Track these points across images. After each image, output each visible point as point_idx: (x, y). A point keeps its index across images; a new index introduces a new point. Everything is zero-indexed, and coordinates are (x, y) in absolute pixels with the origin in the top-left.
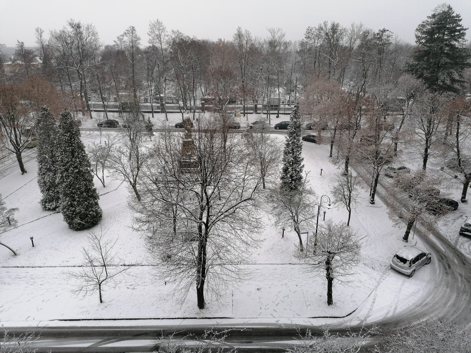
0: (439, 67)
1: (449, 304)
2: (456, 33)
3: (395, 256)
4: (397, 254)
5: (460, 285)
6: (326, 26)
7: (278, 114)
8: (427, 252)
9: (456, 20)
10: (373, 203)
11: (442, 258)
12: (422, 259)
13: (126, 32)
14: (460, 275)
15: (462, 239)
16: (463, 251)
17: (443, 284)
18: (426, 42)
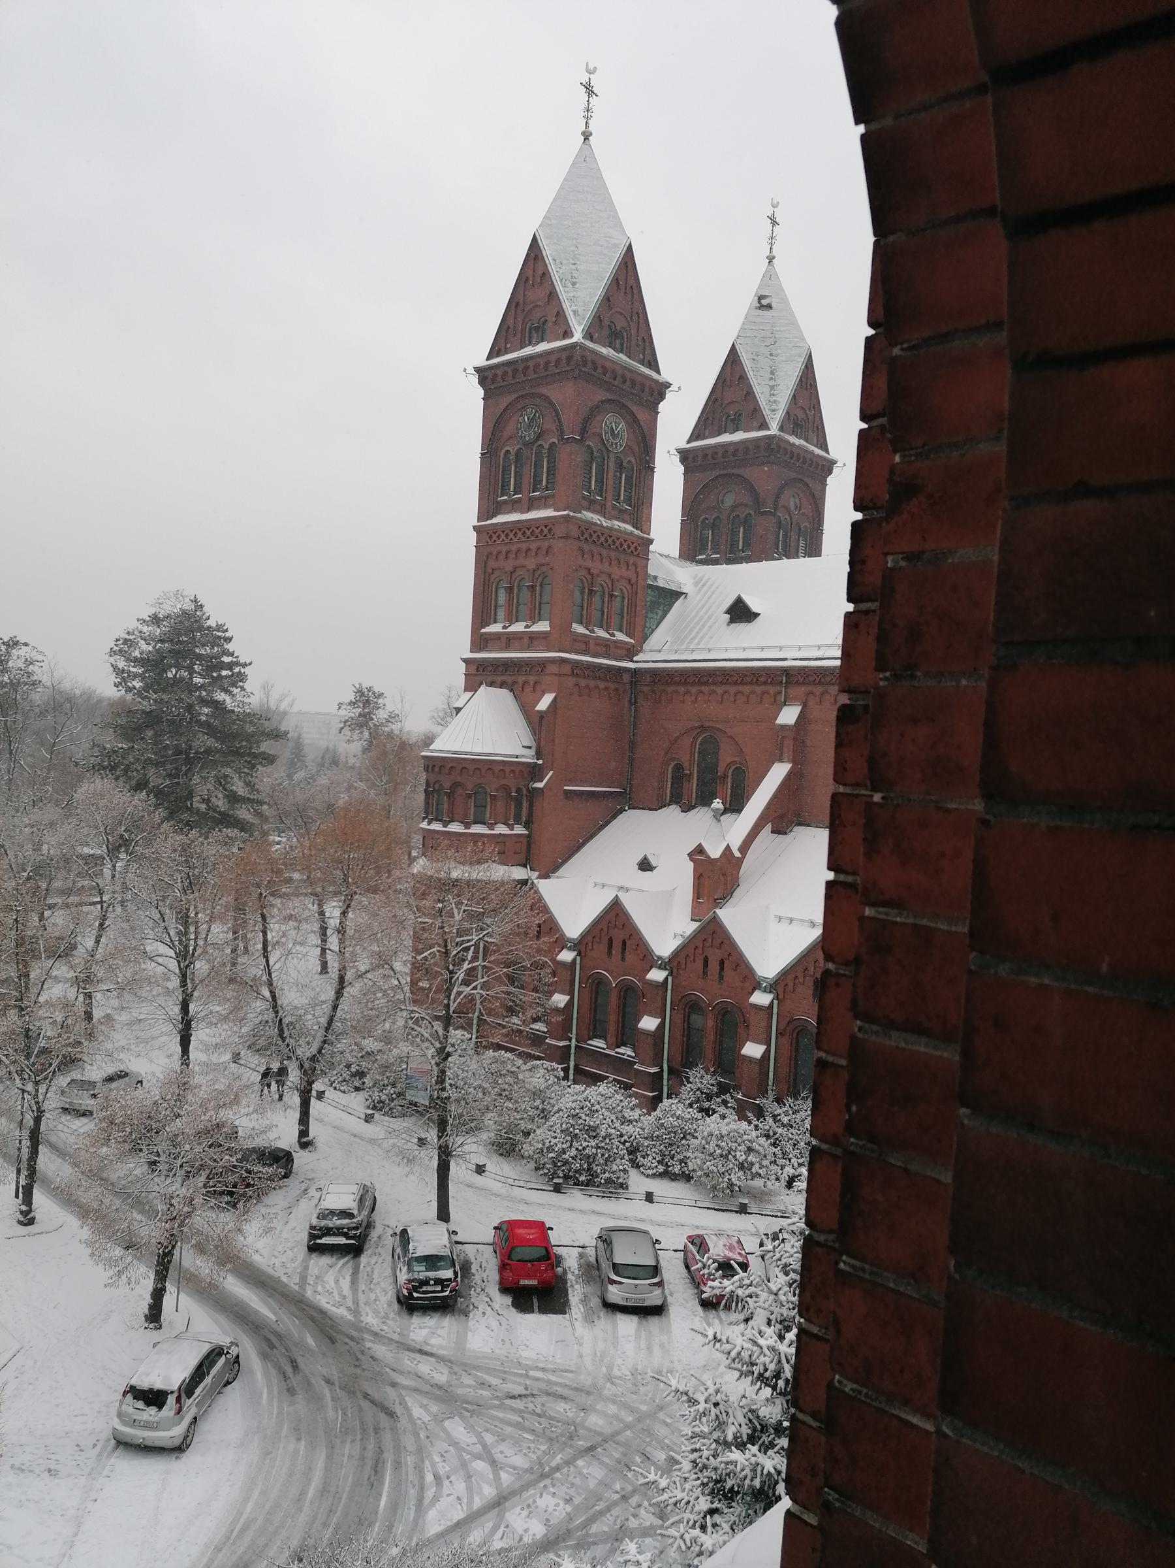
0: (189, 760)
1: (311, 1492)
2: (224, 673)
3: (125, 1393)
4: (133, 1382)
5: (331, 1414)
8: (224, 1341)
9: (218, 637)
10: (31, 1222)
11: (272, 1346)
12: (214, 1371)
14: (328, 1381)
15: (320, 1263)
16: (323, 1302)
17: (284, 1434)
18: (146, 688)
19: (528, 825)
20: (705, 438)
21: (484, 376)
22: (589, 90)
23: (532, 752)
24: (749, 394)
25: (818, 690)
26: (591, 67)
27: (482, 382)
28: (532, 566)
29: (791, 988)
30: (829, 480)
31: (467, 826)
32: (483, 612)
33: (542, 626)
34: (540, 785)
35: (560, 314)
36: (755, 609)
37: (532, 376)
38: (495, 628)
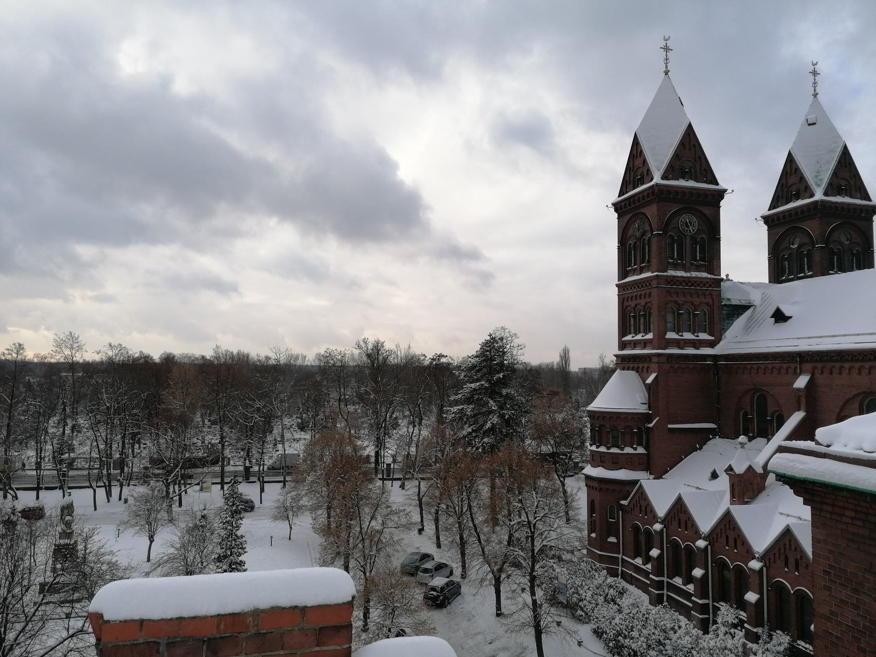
6: (365, 343)
7: (284, 482)
13: (6, 352)
19: (646, 448)
20: (778, 207)
21: (617, 207)
22: (666, 49)
23: (646, 406)
24: (802, 178)
25: (819, 365)
26: (667, 37)
27: (616, 210)
28: (643, 304)
29: (772, 560)
31: (608, 448)
32: (624, 330)
33: (650, 336)
34: (651, 425)
35: (648, 170)
36: (787, 314)
37: (637, 204)
38: (629, 338)
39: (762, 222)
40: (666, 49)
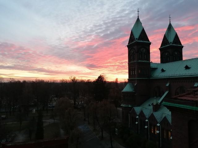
21: (128, 46)
30: (183, 49)
39: (159, 50)
40: (170, 17)
